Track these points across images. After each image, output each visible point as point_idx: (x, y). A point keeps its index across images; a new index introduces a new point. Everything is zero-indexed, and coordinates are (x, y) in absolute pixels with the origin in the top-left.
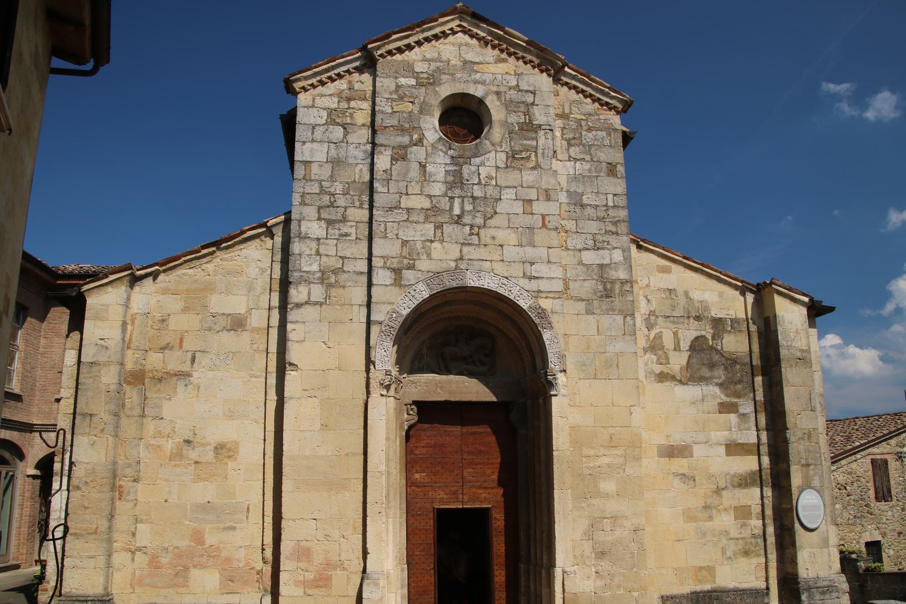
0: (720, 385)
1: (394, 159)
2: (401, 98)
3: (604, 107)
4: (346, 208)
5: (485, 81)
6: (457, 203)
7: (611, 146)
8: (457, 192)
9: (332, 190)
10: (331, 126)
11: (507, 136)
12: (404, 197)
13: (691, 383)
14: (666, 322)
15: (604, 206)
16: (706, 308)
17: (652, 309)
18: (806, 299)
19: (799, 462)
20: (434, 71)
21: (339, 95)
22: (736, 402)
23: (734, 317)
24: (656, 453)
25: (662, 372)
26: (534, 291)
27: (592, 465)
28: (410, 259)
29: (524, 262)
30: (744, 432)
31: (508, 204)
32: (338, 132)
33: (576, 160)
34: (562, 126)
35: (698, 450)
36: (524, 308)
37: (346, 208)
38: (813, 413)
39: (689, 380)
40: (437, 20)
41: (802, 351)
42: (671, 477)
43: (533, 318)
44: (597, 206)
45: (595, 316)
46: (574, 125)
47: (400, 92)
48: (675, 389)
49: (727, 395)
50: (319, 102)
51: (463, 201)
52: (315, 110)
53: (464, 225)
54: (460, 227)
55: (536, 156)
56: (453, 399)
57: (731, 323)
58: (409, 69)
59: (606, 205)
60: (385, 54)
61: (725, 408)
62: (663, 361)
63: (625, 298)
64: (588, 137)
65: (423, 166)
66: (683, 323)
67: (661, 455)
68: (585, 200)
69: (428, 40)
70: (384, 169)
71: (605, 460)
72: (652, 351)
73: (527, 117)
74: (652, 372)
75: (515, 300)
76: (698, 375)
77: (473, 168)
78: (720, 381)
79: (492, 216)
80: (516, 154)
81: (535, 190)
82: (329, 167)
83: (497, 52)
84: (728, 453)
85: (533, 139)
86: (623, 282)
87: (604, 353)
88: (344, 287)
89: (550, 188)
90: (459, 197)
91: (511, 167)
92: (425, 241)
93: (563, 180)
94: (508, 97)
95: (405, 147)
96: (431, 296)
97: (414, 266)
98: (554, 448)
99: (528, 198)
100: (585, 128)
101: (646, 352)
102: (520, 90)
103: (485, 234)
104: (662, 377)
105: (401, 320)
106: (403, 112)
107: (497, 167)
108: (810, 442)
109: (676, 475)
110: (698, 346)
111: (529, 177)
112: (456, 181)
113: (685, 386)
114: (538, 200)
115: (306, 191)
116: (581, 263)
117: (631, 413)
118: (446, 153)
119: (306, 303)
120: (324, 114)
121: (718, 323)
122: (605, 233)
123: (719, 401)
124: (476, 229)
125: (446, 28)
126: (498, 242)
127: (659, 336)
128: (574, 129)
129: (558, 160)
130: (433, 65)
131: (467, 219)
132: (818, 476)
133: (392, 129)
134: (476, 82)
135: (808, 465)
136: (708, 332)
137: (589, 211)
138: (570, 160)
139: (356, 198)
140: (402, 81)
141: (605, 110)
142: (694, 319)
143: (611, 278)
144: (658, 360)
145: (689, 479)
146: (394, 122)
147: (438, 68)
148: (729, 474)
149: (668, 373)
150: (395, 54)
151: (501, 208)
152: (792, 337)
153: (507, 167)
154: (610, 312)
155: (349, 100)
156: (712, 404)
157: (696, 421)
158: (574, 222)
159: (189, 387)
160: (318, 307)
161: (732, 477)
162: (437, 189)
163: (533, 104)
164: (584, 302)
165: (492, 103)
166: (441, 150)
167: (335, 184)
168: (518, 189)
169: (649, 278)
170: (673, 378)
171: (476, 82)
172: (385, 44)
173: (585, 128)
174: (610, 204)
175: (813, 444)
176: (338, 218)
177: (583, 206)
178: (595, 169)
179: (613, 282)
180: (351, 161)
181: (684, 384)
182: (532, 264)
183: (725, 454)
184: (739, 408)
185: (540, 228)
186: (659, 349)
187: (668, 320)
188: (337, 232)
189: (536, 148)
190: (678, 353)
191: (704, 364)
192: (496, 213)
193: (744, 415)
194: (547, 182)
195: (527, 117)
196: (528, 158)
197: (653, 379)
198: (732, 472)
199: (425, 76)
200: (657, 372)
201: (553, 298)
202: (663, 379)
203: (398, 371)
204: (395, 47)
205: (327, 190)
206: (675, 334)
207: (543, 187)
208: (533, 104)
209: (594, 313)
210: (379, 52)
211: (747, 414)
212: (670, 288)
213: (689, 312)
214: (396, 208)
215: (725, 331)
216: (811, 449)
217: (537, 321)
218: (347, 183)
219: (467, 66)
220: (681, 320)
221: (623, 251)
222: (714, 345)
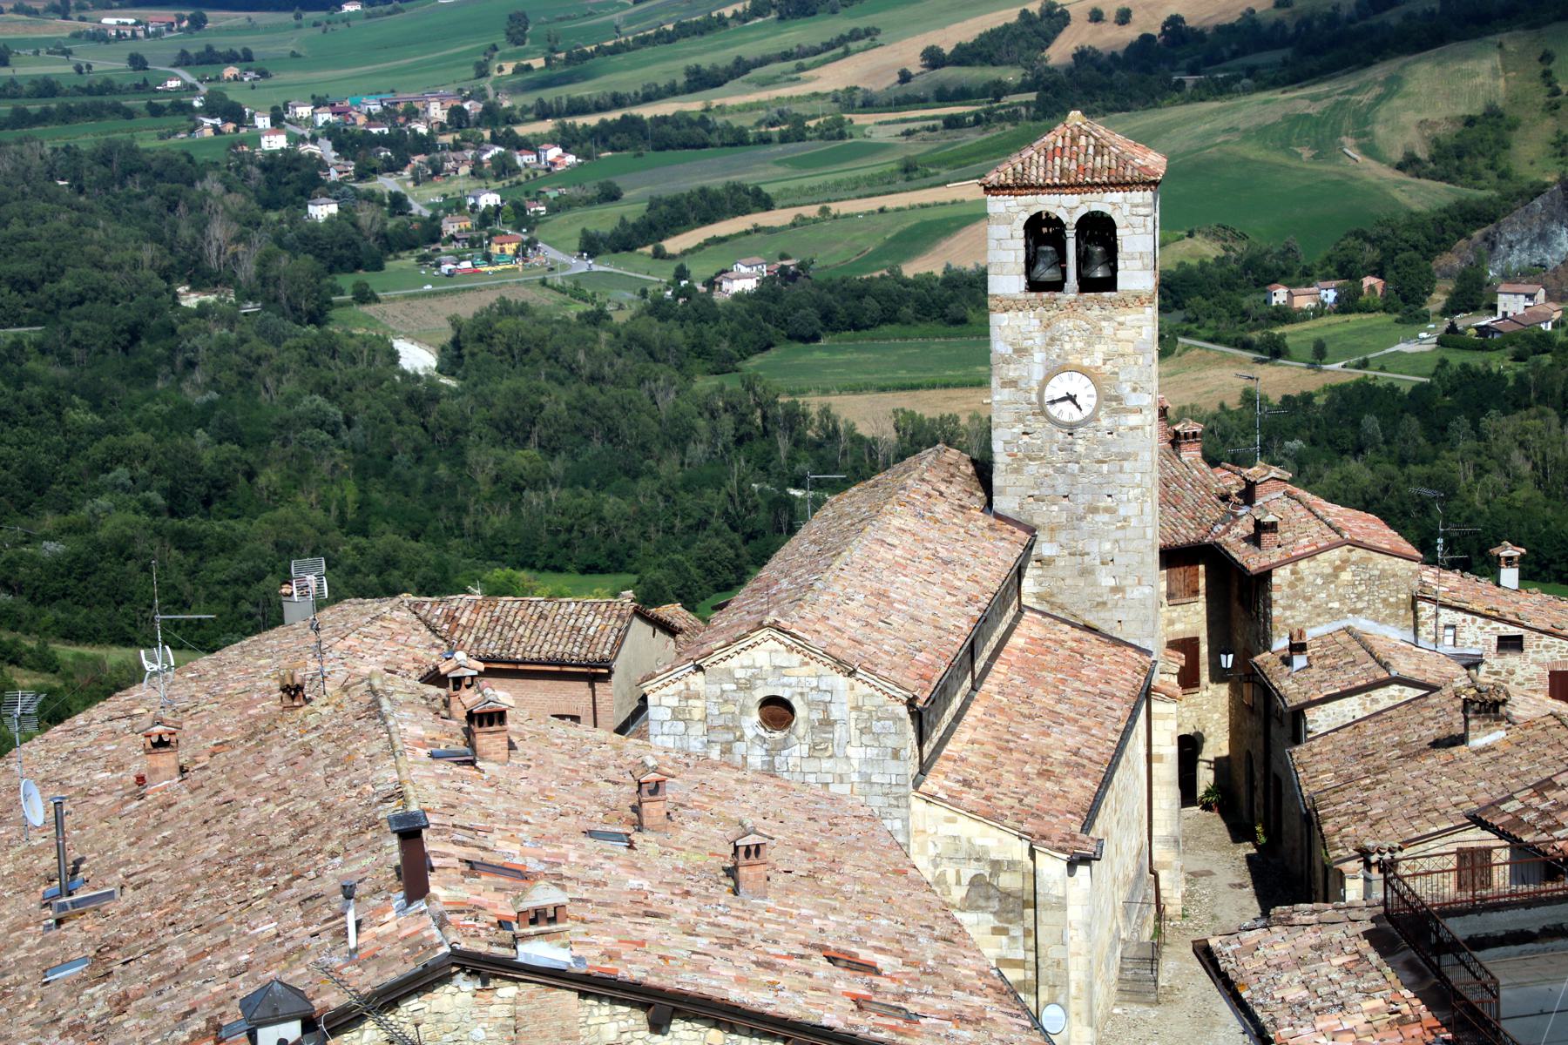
0: (995, 913)
1: (723, 752)
2: (726, 701)
16: (987, 852)
21: (679, 694)
32: (681, 726)
46: (866, 716)
50: (665, 701)
61: (997, 931)
64: (877, 727)
68: (874, 779)
83: (800, 656)
93: (855, 763)
95: (730, 743)
110: (976, 882)
111: (827, 764)
121: (996, 865)
125: (758, 639)
127: (943, 874)
130: (750, 672)
134: (784, 685)
136: (986, 871)
137: (877, 789)
140: (726, 687)
146: (721, 722)
155: (687, 698)
156: (987, 928)
165: (797, 703)
171: (784, 685)
177: (871, 784)
193: (1014, 938)
194: (842, 767)
206: (958, 872)
215: (1000, 870)
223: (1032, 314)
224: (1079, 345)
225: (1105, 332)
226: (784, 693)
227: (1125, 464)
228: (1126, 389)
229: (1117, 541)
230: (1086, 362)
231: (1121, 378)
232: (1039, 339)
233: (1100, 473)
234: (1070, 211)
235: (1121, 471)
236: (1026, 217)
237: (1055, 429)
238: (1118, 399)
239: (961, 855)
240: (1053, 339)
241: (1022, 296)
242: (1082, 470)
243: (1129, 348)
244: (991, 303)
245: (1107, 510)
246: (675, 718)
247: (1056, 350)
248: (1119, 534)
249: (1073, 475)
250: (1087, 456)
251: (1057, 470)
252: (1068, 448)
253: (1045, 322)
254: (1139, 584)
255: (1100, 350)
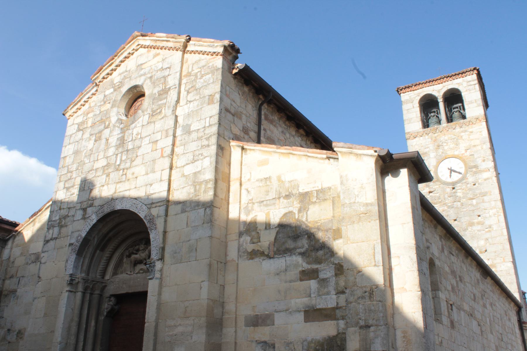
0: (302, 254)
1: (96, 141)
3: (214, 56)
4: (75, 178)
5: (145, 73)
6: (119, 155)
7: (213, 82)
8: (120, 150)
9: (71, 170)
10: (78, 133)
11: (151, 103)
12: (96, 162)
13: (277, 256)
14: (260, 206)
15: (203, 128)
17: (251, 198)
18: (371, 152)
19: (358, 323)
20: (123, 79)
22: (317, 268)
23: (320, 188)
24: (243, 323)
25: (253, 250)
26: (149, 204)
27: (171, 333)
28: (92, 201)
29: (147, 185)
30: (324, 296)
31: (146, 148)
33: (190, 102)
34: (186, 81)
35: (279, 319)
36: (142, 217)
37: (75, 178)
38: (376, 268)
39: (275, 253)
40: (124, 48)
41: (367, 205)
42: (254, 344)
43: (146, 222)
44: (199, 130)
45: (186, 213)
47: (105, 100)
48: (263, 263)
49: (308, 263)
51: (122, 155)
52: (73, 126)
53: (120, 170)
54: (118, 172)
55: (165, 109)
56: (130, 291)
57: (317, 193)
58: (112, 83)
59: (204, 127)
60: (102, 80)
62: (255, 240)
63: (208, 194)
65: (107, 140)
66: (274, 204)
67: (247, 325)
69: (122, 62)
70: (90, 149)
71: (180, 329)
72: (247, 234)
73: (164, 85)
74: (246, 251)
75: (138, 214)
76: (283, 248)
77: (130, 131)
78: (302, 250)
79: (135, 159)
80: (154, 113)
81: (161, 132)
82: (73, 156)
84: (307, 319)
85: (164, 99)
86: (207, 182)
87: (189, 241)
88: (66, 226)
89: (169, 128)
90: (120, 153)
91: (150, 122)
92: (101, 186)
94: (156, 77)
95: (101, 132)
96: (99, 221)
97: (93, 205)
98: (146, 321)
99: (155, 140)
100: (199, 77)
101: (243, 235)
102: (163, 70)
103: (129, 172)
104: (253, 254)
105: (81, 240)
106: (104, 111)
107: (143, 126)
108: (371, 301)
109: (258, 342)
112: (122, 141)
113: (272, 260)
114: (161, 139)
115: (62, 174)
116: (183, 175)
117: (201, 288)
118: (119, 127)
119: (51, 239)
120: (76, 126)
122: (201, 148)
123: (301, 269)
124: (125, 170)
125: (130, 50)
126: (135, 176)
128: (192, 81)
129: (180, 106)
130: (122, 76)
131: (122, 167)
132: (380, 338)
133: (97, 123)
134: (141, 75)
135: (368, 327)
137: (194, 135)
138: (187, 104)
139: (80, 171)
140: (107, 92)
141: (215, 58)
142: (284, 198)
143: (200, 181)
144: (251, 240)
145: (269, 346)
146: (99, 118)
147: (125, 76)
148: (306, 340)
149: (258, 250)
150: (107, 77)
151: (140, 152)
152: (356, 193)
153: (148, 123)
154: (196, 208)
155: (88, 114)
156: (294, 273)
157: (279, 291)
158: (183, 146)
159: (15, 298)
160: (54, 241)
161: (310, 343)
162: (111, 151)
163: (168, 75)
164: (181, 204)
166: (117, 127)
167: (74, 165)
168: (151, 136)
169: (251, 173)
170: (262, 254)
172: (100, 74)
173: (199, 77)
174: (207, 125)
175: (375, 303)
176: (71, 185)
178: (201, 103)
179: (201, 183)
180: (82, 149)
181: (273, 258)
182: (151, 185)
183: (303, 320)
184: (319, 273)
185: (159, 158)
186: (253, 231)
187: (262, 204)
188: (69, 193)
189: (166, 104)
190: (268, 231)
191: (289, 237)
192: (137, 156)
195: (164, 85)
196: (160, 112)
197: (246, 257)
198: (309, 339)
199: (118, 84)
200: (250, 250)
201: (159, 206)
202: (253, 256)
203: (100, 275)
204: (105, 74)
205: (70, 170)
207: (165, 129)
208: (168, 75)
209: (186, 211)
210: (99, 81)
211: (326, 279)
212: (266, 177)
213: (280, 193)
214: (91, 171)
216: (373, 308)
217: (148, 225)
218: (79, 163)
219: (139, 68)
220: (274, 201)
221: (211, 157)
222: (300, 218)
223: (427, 137)
224: (452, 146)
225: (464, 137)
226: (139, 82)
227: (486, 198)
228: (479, 161)
229: (487, 239)
230: (456, 153)
231: (476, 156)
232: (431, 147)
233: (472, 205)
234: (439, 91)
235: (483, 201)
236: (419, 98)
237: (445, 186)
238: (476, 167)
239: (272, 195)
240: (439, 146)
241: (422, 130)
242: (462, 204)
243: (477, 142)
244: (407, 136)
245: (478, 223)
246: (79, 130)
247: (440, 151)
248: (488, 235)
249: (457, 208)
250: (464, 198)
251: (449, 207)
252: (453, 195)
253: (434, 139)
254: (504, 261)
255: (463, 145)
